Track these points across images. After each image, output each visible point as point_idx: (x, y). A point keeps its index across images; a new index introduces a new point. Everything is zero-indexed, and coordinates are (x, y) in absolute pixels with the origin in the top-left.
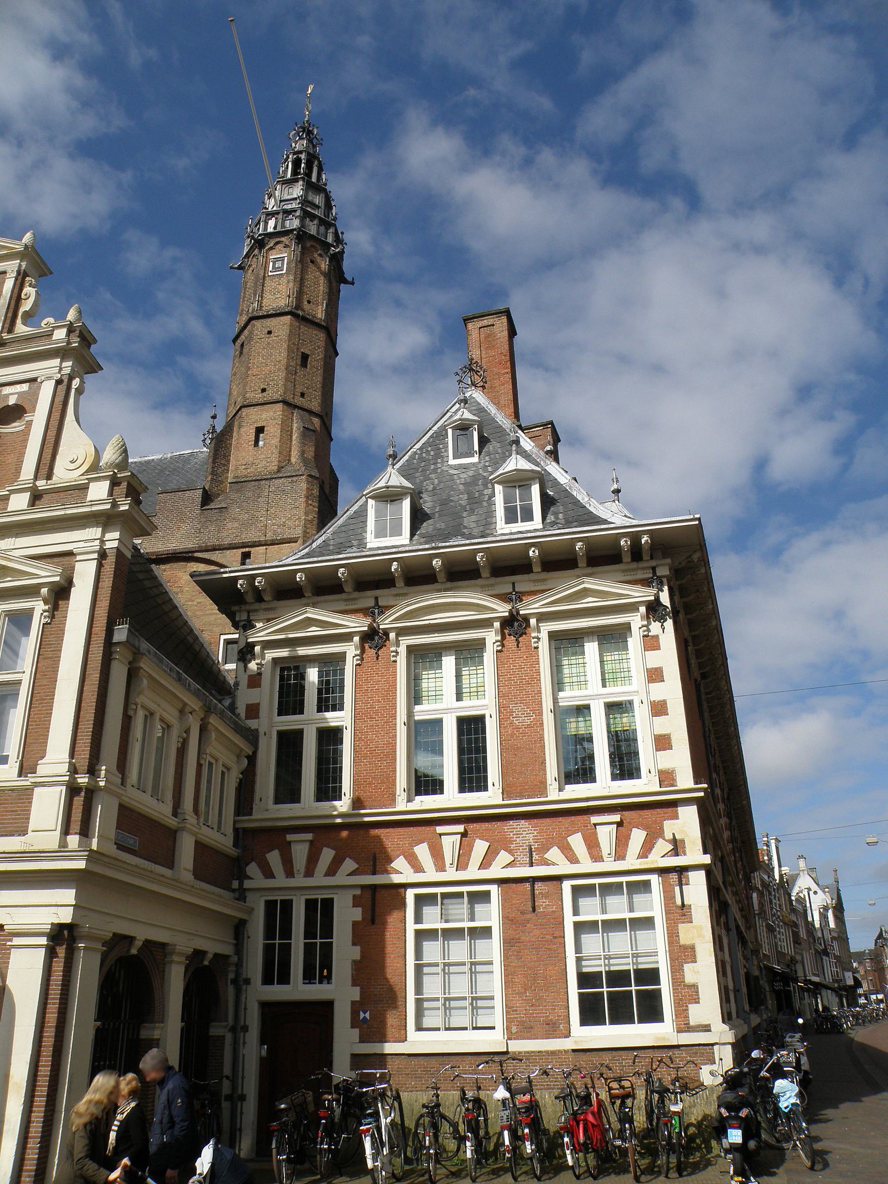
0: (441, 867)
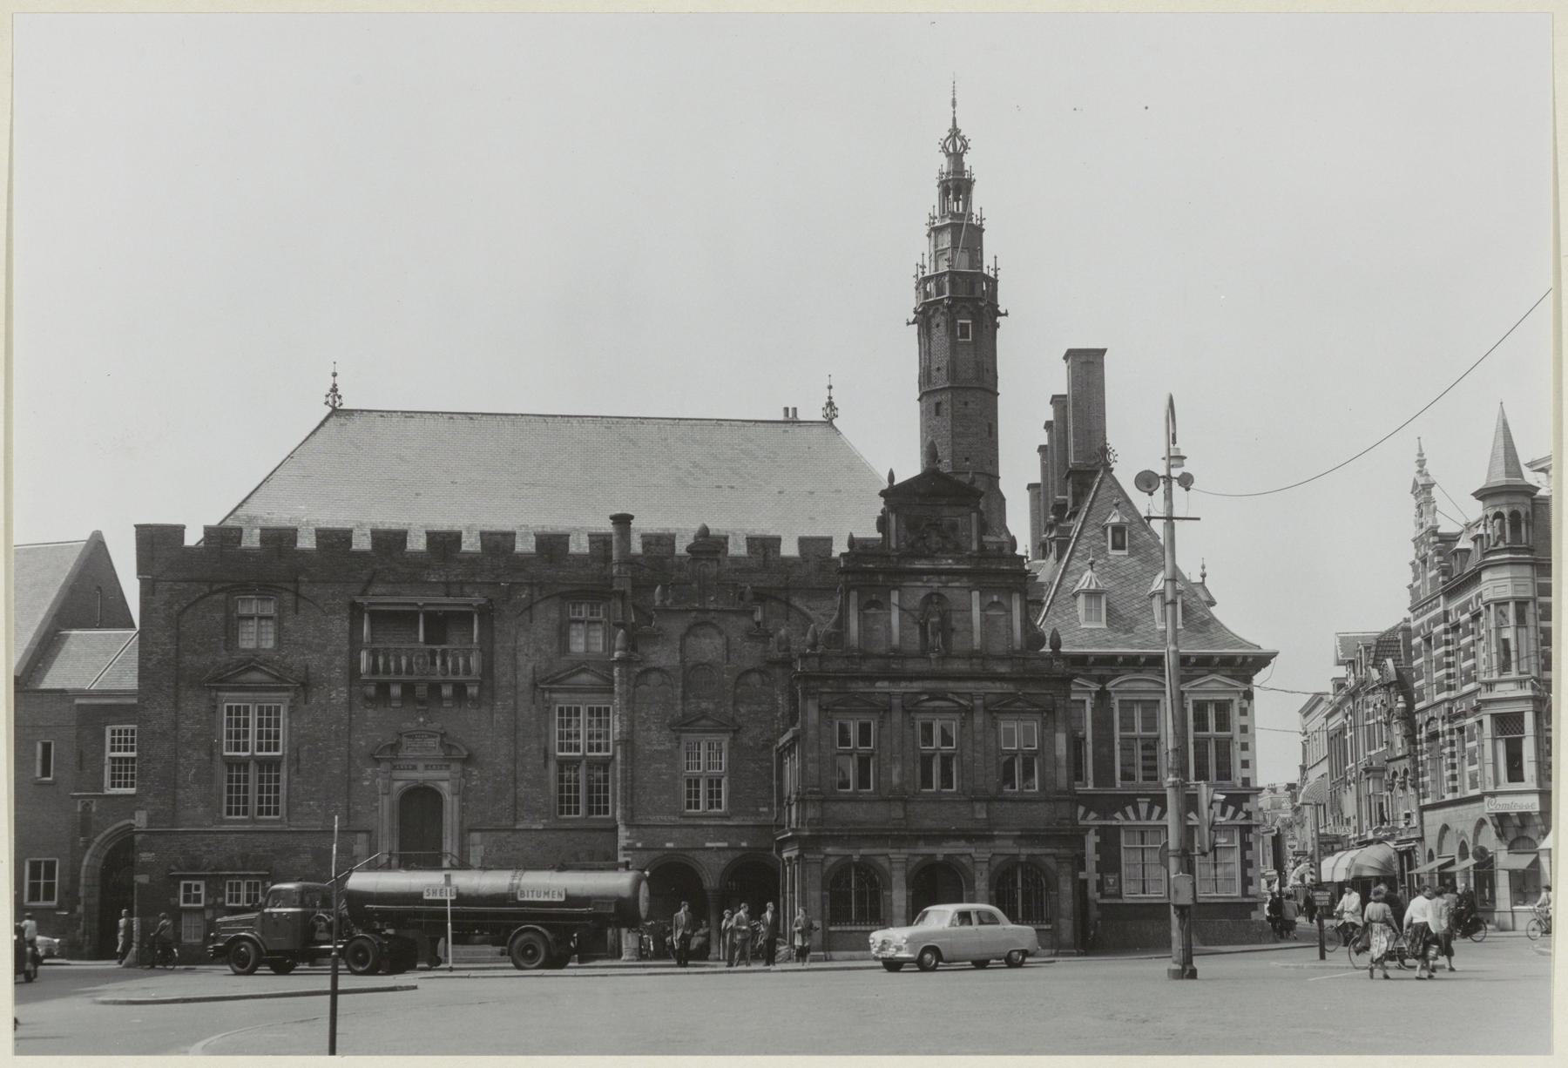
0: (1138, 818)
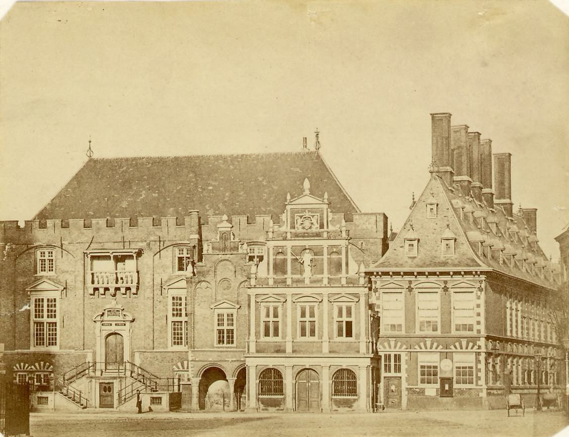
0: (426, 348)
